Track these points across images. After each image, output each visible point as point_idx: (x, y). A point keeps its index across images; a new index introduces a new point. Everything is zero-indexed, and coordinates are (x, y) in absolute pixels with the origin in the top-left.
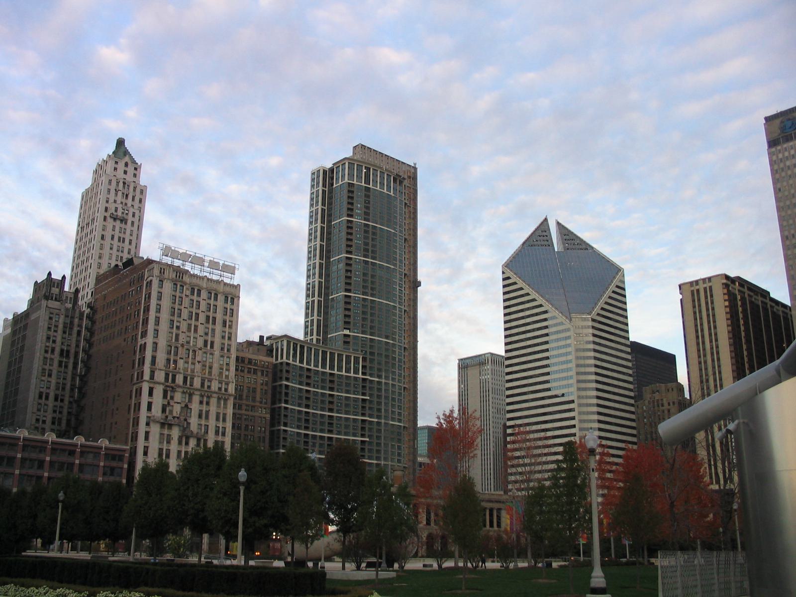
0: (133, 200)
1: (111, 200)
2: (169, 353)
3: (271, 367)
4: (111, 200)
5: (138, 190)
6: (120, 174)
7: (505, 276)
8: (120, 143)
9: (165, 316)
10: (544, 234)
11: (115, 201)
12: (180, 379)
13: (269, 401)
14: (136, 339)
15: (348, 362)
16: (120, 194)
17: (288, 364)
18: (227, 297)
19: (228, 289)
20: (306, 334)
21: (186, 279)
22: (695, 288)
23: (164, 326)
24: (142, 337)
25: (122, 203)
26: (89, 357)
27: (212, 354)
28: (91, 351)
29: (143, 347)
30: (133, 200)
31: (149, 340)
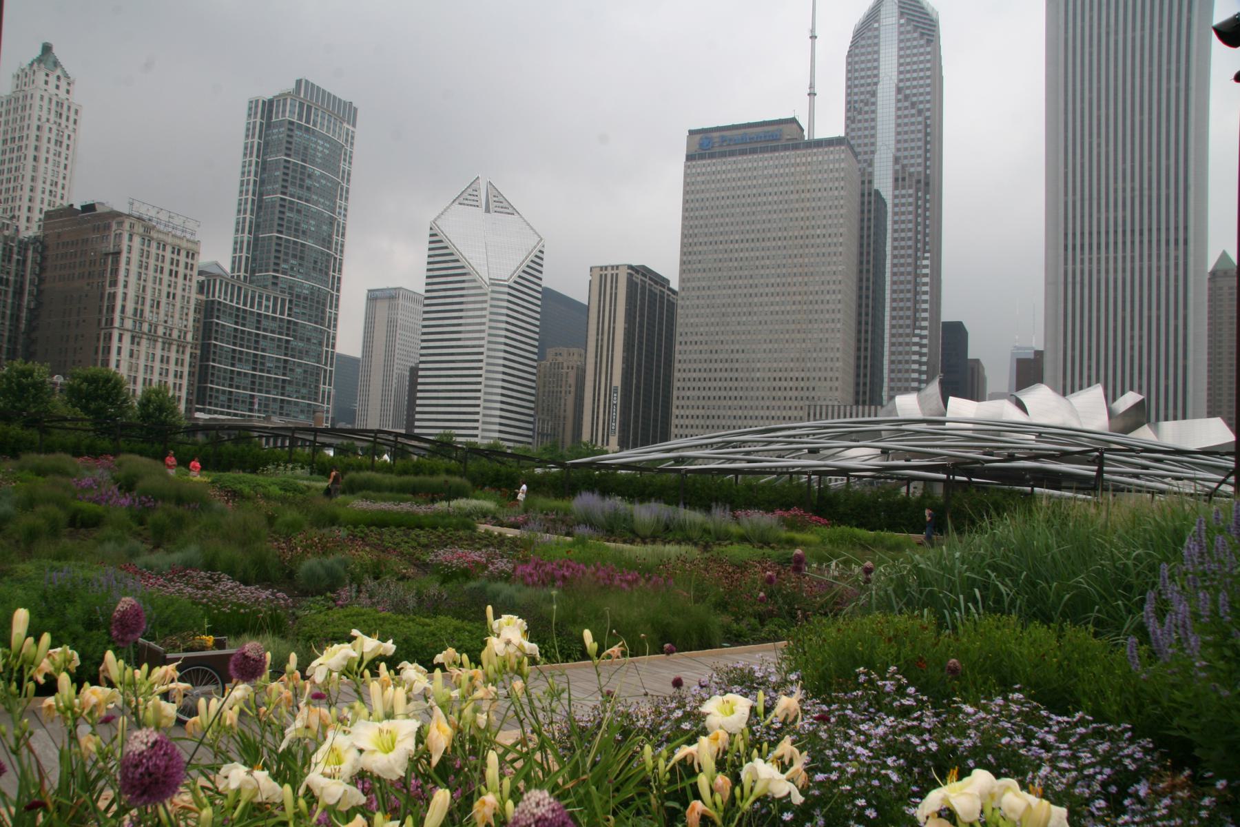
1: (44, 119)
2: (137, 303)
3: (203, 304)
4: (44, 119)
5: (72, 111)
7: (433, 232)
8: (47, 49)
9: (134, 268)
10: (475, 193)
11: (48, 120)
12: (146, 327)
13: (200, 337)
14: (103, 287)
15: (283, 306)
16: (53, 112)
17: (219, 303)
18: (188, 253)
19: (190, 245)
20: (233, 269)
21: (154, 234)
22: (604, 272)
23: (133, 279)
24: (110, 286)
25: (55, 122)
26: (40, 292)
27: (174, 305)
28: (42, 287)
29: (113, 296)
31: (120, 290)
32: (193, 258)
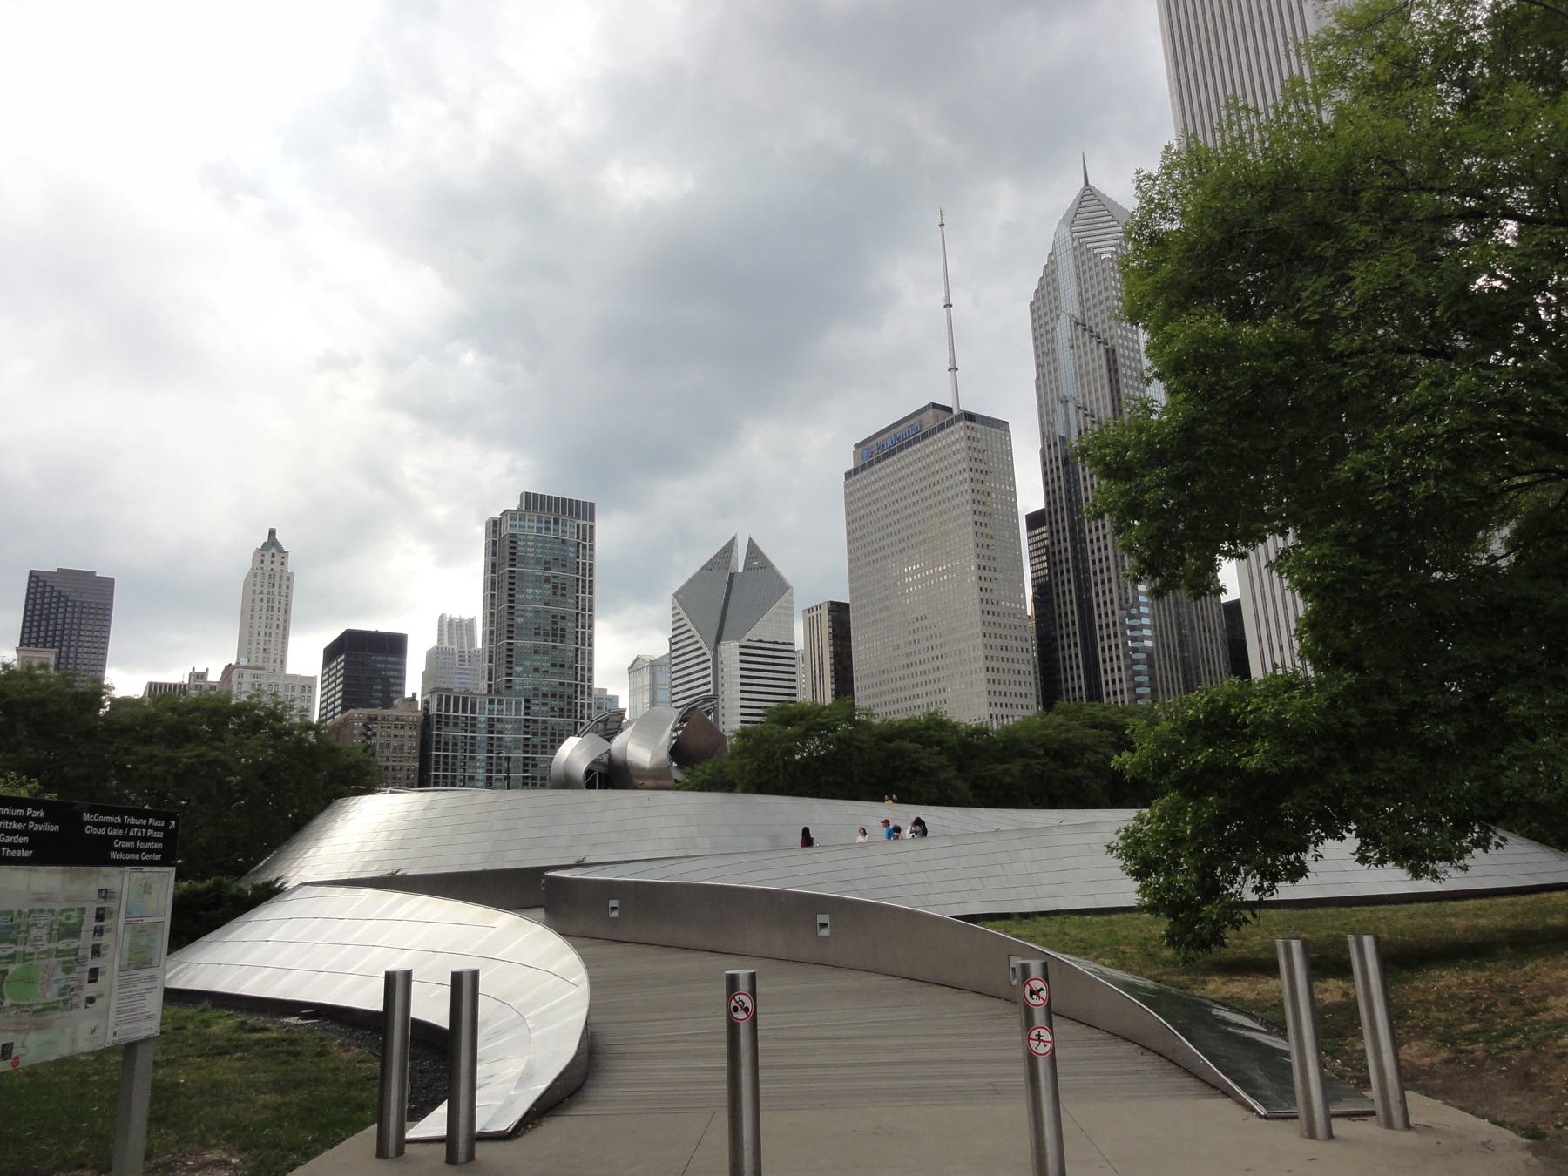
0: (280, 587)
4: (259, 592)
5: (285, 578)
6: (267, 564)
8: (272, 533)
30: (280, 587)
32: (310, 691)
